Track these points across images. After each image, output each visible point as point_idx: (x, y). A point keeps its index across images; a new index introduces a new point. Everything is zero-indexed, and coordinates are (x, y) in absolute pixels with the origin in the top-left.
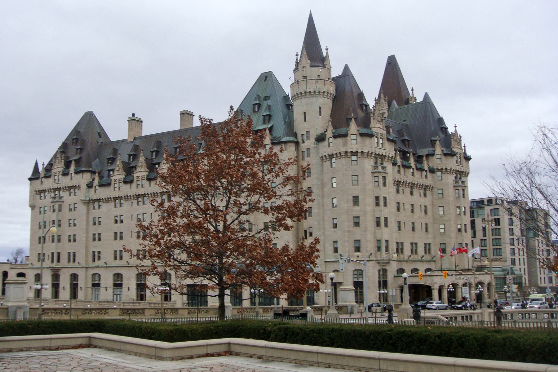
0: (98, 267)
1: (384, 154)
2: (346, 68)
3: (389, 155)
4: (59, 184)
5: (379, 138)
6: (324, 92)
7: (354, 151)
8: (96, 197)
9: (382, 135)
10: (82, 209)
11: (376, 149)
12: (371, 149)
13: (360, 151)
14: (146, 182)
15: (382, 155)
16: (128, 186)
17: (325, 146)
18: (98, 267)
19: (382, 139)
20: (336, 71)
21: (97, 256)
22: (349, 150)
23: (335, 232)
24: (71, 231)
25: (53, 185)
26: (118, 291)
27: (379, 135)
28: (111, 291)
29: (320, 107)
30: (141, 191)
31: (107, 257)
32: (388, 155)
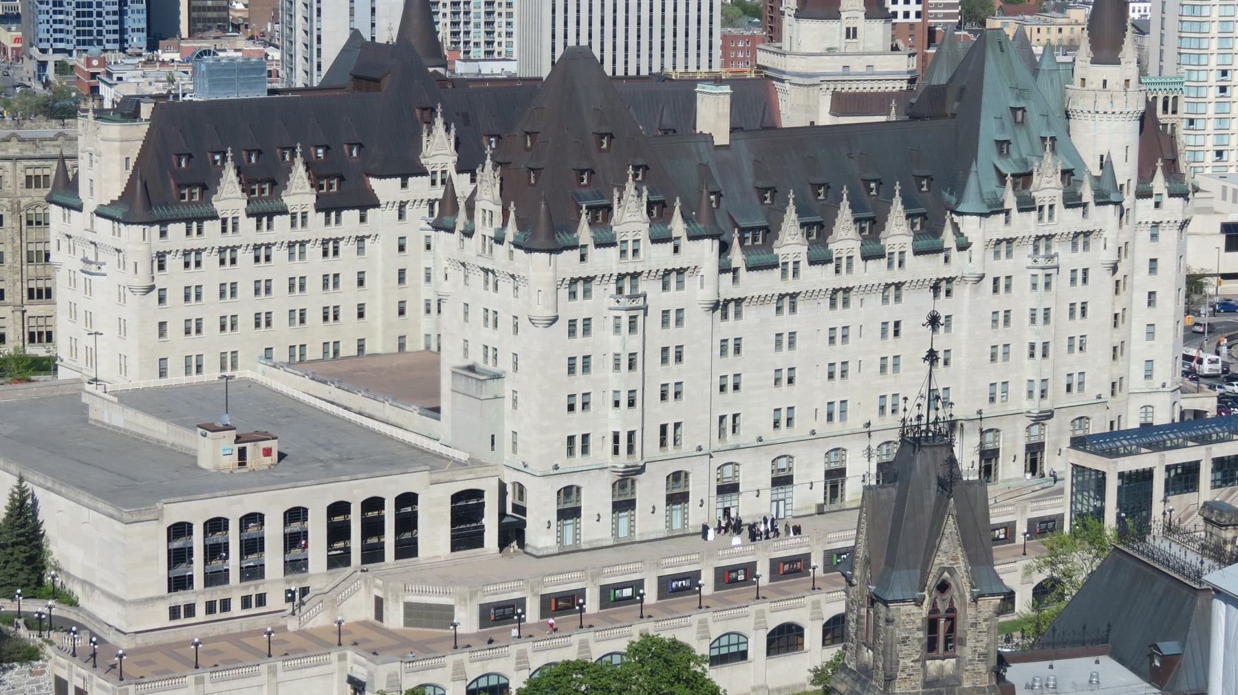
0: (737, 448)
4: (642, 264)
8: (735, 293)
10: (696, 319)
14: (858, 262)
16: (817, 269)
17: (1148, 206)
18: (737, 448)
21: (730, 423)
23: (1151, 346)
24: (671, 374)
25: (621, 266)
26: (781, 492)
28: (767, 495)
30: (844, 281)
31: (756, 423)
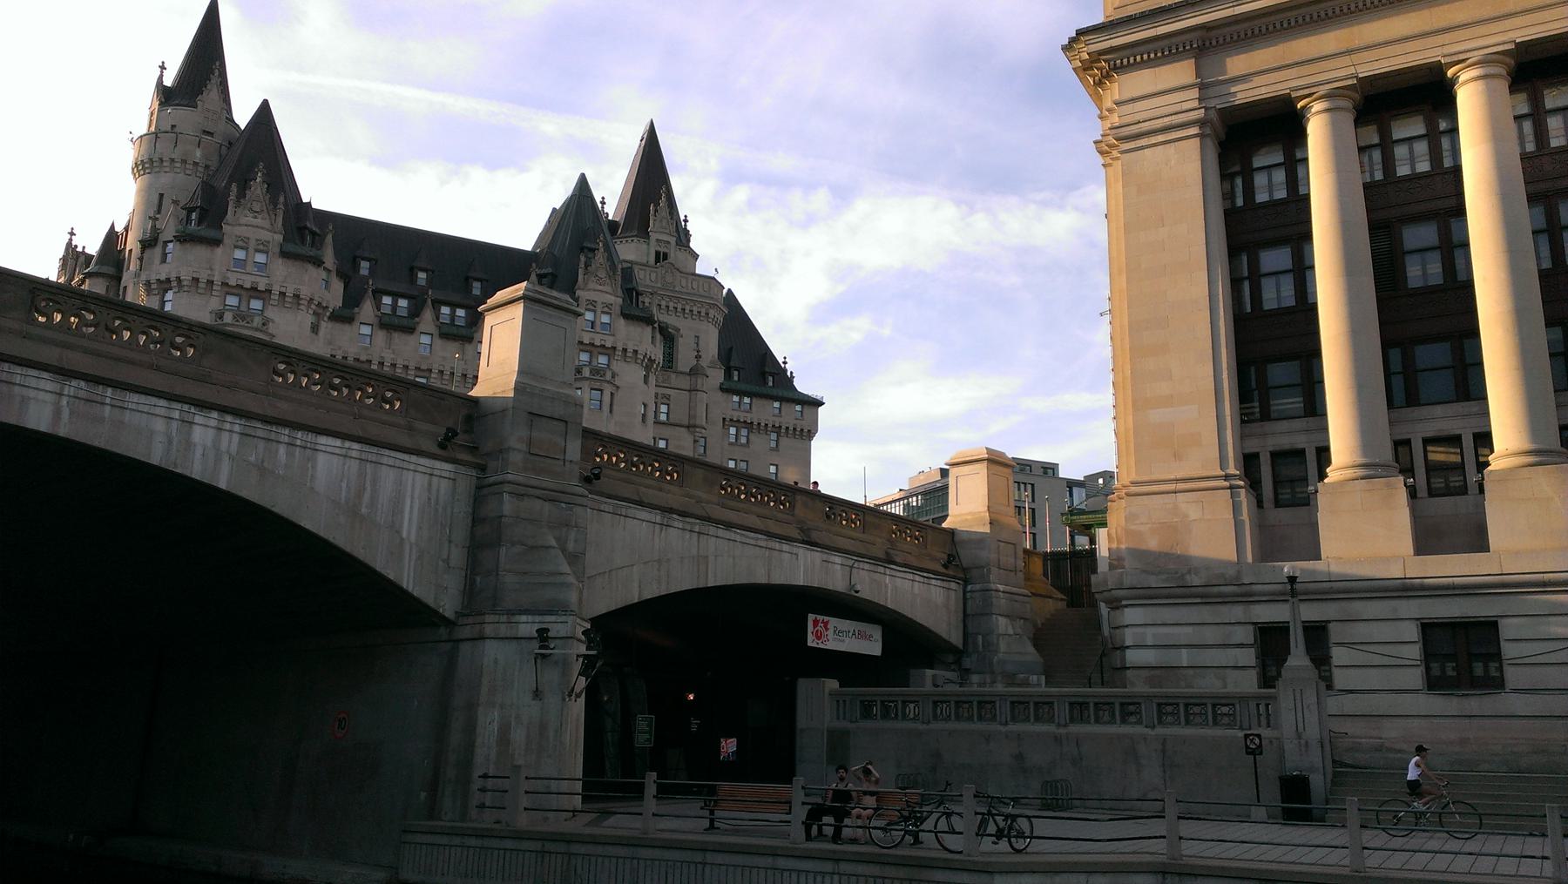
1: (261, 287)
2: (265, 107)
3: (283, 290)
5: (251, 250)
6: (172, 160)
7: (163, 278)
9: (265, 243)
11: (229, 274)
12: (209, 272)
13: (173, 276)
15: (254, 289)
19: (267, 253)
20: (243, 115)
22: (153, 278)
27: (252, 244)
29: (161, 195)
32: (276, 290)
